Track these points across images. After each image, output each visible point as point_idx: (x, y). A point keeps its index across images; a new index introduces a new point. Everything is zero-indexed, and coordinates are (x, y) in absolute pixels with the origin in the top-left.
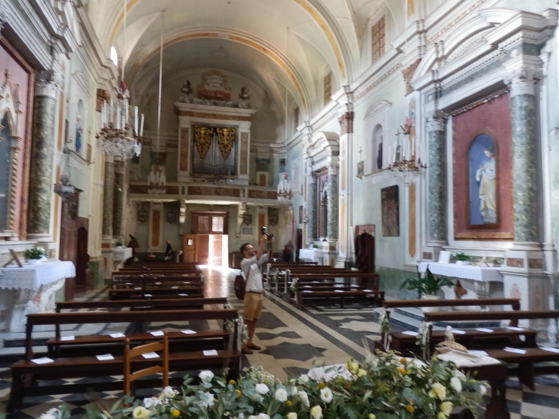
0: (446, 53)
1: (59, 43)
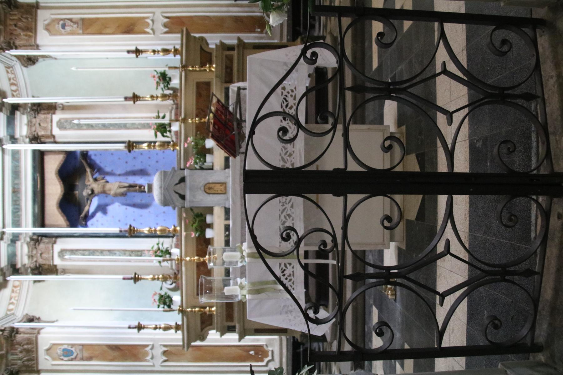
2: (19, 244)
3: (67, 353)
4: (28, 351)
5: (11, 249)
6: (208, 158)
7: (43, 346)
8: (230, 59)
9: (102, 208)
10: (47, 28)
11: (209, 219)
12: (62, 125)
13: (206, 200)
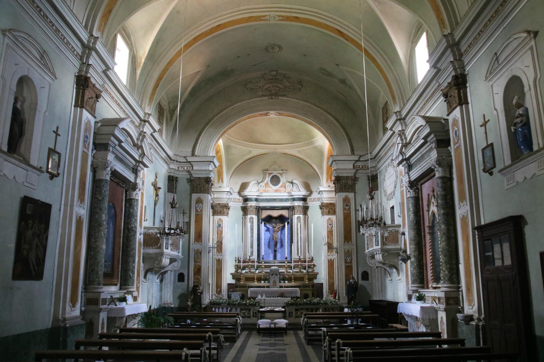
0: (408, 139)
1: (141, 165)
3: (219, 226)
4: (220, 213)
6: (283, 282)
7: (222, 217)
8: (309, 287)
9: (268, 230)
11: (266, 282)
12: (299, 218)
13: (272, 281)
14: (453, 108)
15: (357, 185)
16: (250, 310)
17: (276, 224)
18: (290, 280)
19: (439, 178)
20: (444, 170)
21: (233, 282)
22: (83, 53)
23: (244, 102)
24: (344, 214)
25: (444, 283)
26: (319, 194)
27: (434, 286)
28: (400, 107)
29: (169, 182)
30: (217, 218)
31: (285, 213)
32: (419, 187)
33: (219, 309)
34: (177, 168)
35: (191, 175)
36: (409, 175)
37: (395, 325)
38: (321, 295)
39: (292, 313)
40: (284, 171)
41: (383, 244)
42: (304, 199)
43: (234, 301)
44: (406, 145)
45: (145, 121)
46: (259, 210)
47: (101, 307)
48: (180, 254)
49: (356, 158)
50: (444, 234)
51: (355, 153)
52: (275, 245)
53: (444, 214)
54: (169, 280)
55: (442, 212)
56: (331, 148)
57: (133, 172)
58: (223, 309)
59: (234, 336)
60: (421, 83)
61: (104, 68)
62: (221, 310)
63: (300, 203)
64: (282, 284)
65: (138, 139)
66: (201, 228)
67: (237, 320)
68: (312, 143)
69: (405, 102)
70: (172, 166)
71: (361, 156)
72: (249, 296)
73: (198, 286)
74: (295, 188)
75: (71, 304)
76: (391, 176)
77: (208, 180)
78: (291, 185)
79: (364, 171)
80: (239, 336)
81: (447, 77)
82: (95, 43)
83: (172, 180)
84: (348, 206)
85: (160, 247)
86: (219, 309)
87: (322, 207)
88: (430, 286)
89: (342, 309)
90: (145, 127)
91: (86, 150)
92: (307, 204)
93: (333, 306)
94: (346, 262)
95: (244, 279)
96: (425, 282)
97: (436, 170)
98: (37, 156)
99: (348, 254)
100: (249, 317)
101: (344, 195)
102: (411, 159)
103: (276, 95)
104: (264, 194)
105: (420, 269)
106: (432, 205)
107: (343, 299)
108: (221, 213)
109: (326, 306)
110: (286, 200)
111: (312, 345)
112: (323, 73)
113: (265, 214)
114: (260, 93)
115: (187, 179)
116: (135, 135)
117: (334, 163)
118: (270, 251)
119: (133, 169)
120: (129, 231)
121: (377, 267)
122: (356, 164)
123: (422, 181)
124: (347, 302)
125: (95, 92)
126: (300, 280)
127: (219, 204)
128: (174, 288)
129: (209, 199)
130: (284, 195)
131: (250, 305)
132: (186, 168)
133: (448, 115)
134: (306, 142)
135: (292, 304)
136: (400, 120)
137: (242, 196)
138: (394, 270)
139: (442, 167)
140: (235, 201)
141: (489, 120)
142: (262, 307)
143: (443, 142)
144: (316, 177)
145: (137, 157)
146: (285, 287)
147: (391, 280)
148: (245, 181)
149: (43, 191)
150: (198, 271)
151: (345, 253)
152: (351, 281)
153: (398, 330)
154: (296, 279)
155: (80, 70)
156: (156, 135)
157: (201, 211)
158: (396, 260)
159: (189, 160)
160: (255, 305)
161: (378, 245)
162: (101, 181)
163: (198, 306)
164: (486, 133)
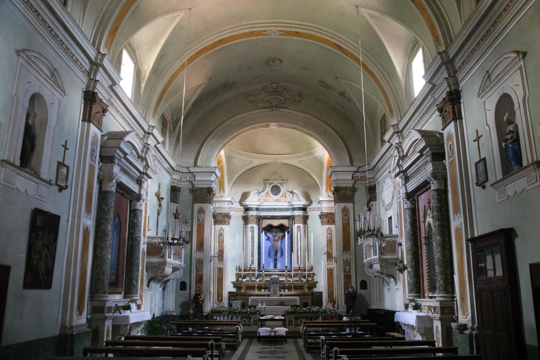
1: (145, 176)
2: (256, 212)
3: (221, 235)
4: (222, 222)
5: (254, 209)
6: (283, 290)
7: (223, 227)
8: (309, 295)
9: (268, 239)
10: (329, 228)
11: (267, 290)
12: (298, 227)
13: (272, 290)
14: (447, 123)
15: (355, 196)
16: (250, 318)
17: (276, 233)
18: (290, 288)
19: (434, 190)
20: (439, 183)
21: (234, 290)
22: (91, 69)
23: (245, 114)
24: (343, 224)
25: (440, 292)
26: (319, 203)
27: (430, 295)
28: (398, 120)
29: (171, 192)
30: (218, 227)
31: (285, 222)
32: (416, 198)
33: (220, 317)
34: (179, 179)
35: (193, 185)
36: (406, 187)
37: (392, 334)
38: (320, 304)
39: (292, 321)
40: (284, 180)
41: (381, 254)
42: (304, 209)
43: (235, 310)
44: (402, 158)
45: (149, 133)
46: (260, 219)
47: (107, 315)
48: (182, 263)
49: (355, 169)
50: (439, 245)
51: (355, 164)
52: (275, 254)
53: (439, 225)
54: (171, 289)
55: (437, 224)
56: (330, 159)
57: (137, 183)
58: (224, 317)
59: (235, 343)
60: (418, 97)
61: (110, 83)
62: (222, 318)
63: (300, 213)
64: (282, 292)
65: (142, 151)
66: (203, 238)
67: (238, 328)
68: (312, 153)
69: (403, 115)
70: (175, 177)
71: (360, 167)
72: (250, 304)
73: (199, 295)
74: (295, 198)
75: (77, 312)
76: (389, 187)
77: (210, 191)
78: (291, 195)
79: (363, 182)
80: (240, 344)
81: (442, 93)
82: (102, 60)
83: (174, 191)
84: (347, 216)
85: (163, 256)
86: (220, 317)
87: (321, 216)
88: (426, 295)
89: (341, 317)
90: (149, 139)
91: (93, 163)
92: (307, 213)
93: (332, 315)
94: (345, 271)
95: (245, 287)
96: (422, 292)
97: (431, 182)
98: (47, 170)
99: (347, 263)
100: (250, 325)
101: (342, 205)
102: (408, 172)
103: (277, 107)
104: (265, 204)
105: (416, 279)
106: (428, 216)
107: (342, 308)
108: (222, 222)
109: (326, 315)
110: (287, 210)
111: (310, 353)
112: (322, 86)
113: (265, 223)
114: (261, 105)
115: (189, 189)
116: (139, 147)
117: (333, 174)
118: (271, 260)
119: (137, 180)
120: (134, 241)
121: (375, 277)
122: (354, 175)
123: (419, 193)
124: (345, 310)
125: (102, 107)
126: (300, 289)
127: (220, 213)
128: (176, 296)
129: (210, 209)
130: (284, 204)
131: (250, 313)
132: (188, 178)
133: (443, 129)
134: (306, 153)
135: (292, 313)
136: (397, 132)
137: (243, 206)
138: (392, 279)
139: (437, 180)
140: (236, 210)
141: (482, 136)
142: (262, 316)
143: (438, 156)
144: (316, 187)
145: (141, 169)
146: (285, 296)
147: (389, 289)
148: (247, 190)
149: (53, 203)
150: (200, 279)
151: (344, 262)
152: (350, 290)
153: (394, 338)
154: (296, 288)
155: (88, 86)
156: (160, 146)
157: (203, 220)
158: (394, 270)
159: (191, 171)
160: (256, 313)
161: (376, 255)
162: (107, 192)
163: (200, 314)
164: (479, 148)
